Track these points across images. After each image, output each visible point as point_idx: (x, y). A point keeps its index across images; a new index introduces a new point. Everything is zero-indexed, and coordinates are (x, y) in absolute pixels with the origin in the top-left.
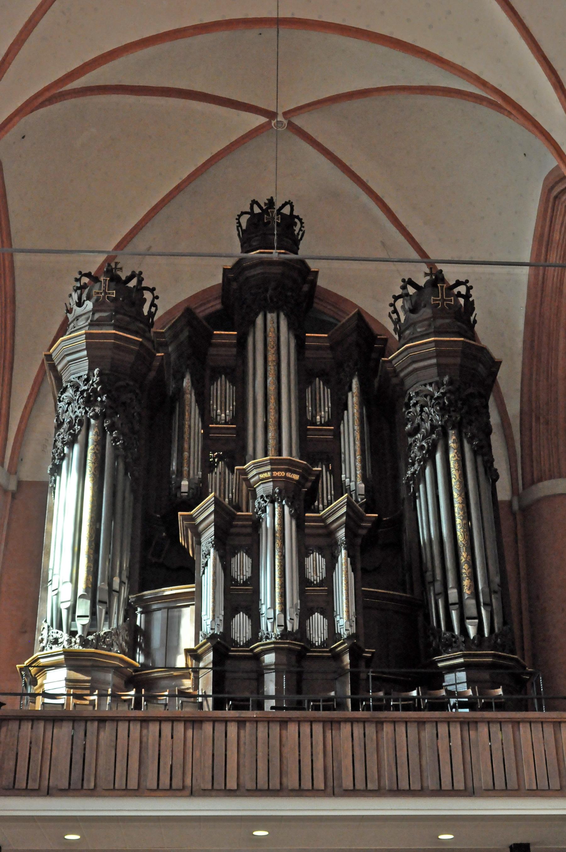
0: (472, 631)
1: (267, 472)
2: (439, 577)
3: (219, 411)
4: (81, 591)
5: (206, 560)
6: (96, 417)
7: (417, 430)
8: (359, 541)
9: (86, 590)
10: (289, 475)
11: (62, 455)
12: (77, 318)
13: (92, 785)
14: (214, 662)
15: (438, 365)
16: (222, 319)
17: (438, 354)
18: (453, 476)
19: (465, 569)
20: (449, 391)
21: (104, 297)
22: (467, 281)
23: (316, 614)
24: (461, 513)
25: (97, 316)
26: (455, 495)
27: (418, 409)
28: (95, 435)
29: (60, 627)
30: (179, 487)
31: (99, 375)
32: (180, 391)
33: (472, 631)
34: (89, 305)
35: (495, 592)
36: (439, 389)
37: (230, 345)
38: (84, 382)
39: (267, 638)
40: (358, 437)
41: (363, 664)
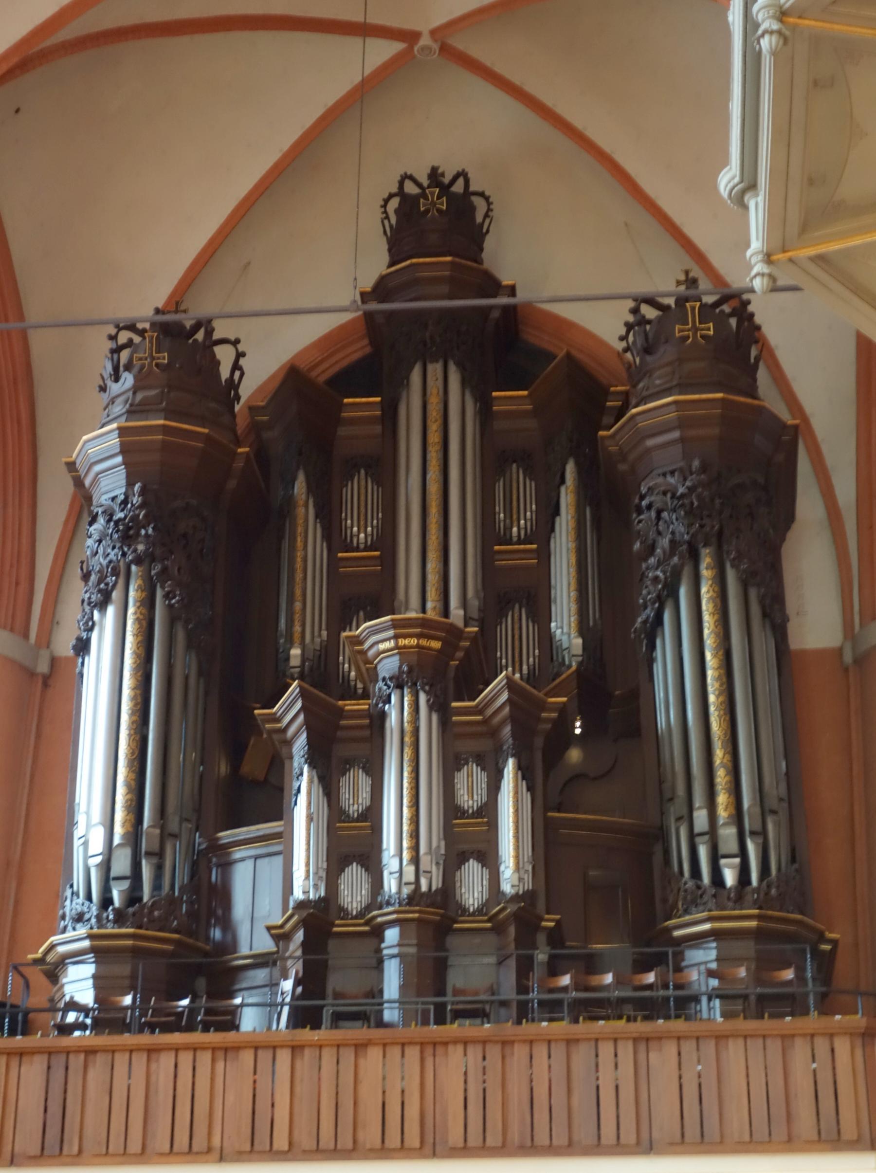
0: (730, 877)
1: (388, 639)
2: (681, 790)
3: (355, 529)
4: (117, 840)
6: (138, 561)
7: (651, 549)
8: (539, 742)
9: (125, 836)
10: (424, 642)
11: (90, 623)
13: (75, 1149)
14: (304, 944)
15: (682, 440)
16: (351, 380)
17: (682, 424)
19: (721, 776)
21: (150, 364)
23: (471, 861)
24: (717, 685)
25: (139, 396)
26: (708, 656)
27: (653, 514)
28: (137, 591)
29: (89, 898)
30: (288, 659)
31: (142, 492)
33: (730, 877)
34: (128, 379)
35: (774, 812)
36: (685, 479)
38: (120, 505)
39: (388, 903)
40: (573, 560)
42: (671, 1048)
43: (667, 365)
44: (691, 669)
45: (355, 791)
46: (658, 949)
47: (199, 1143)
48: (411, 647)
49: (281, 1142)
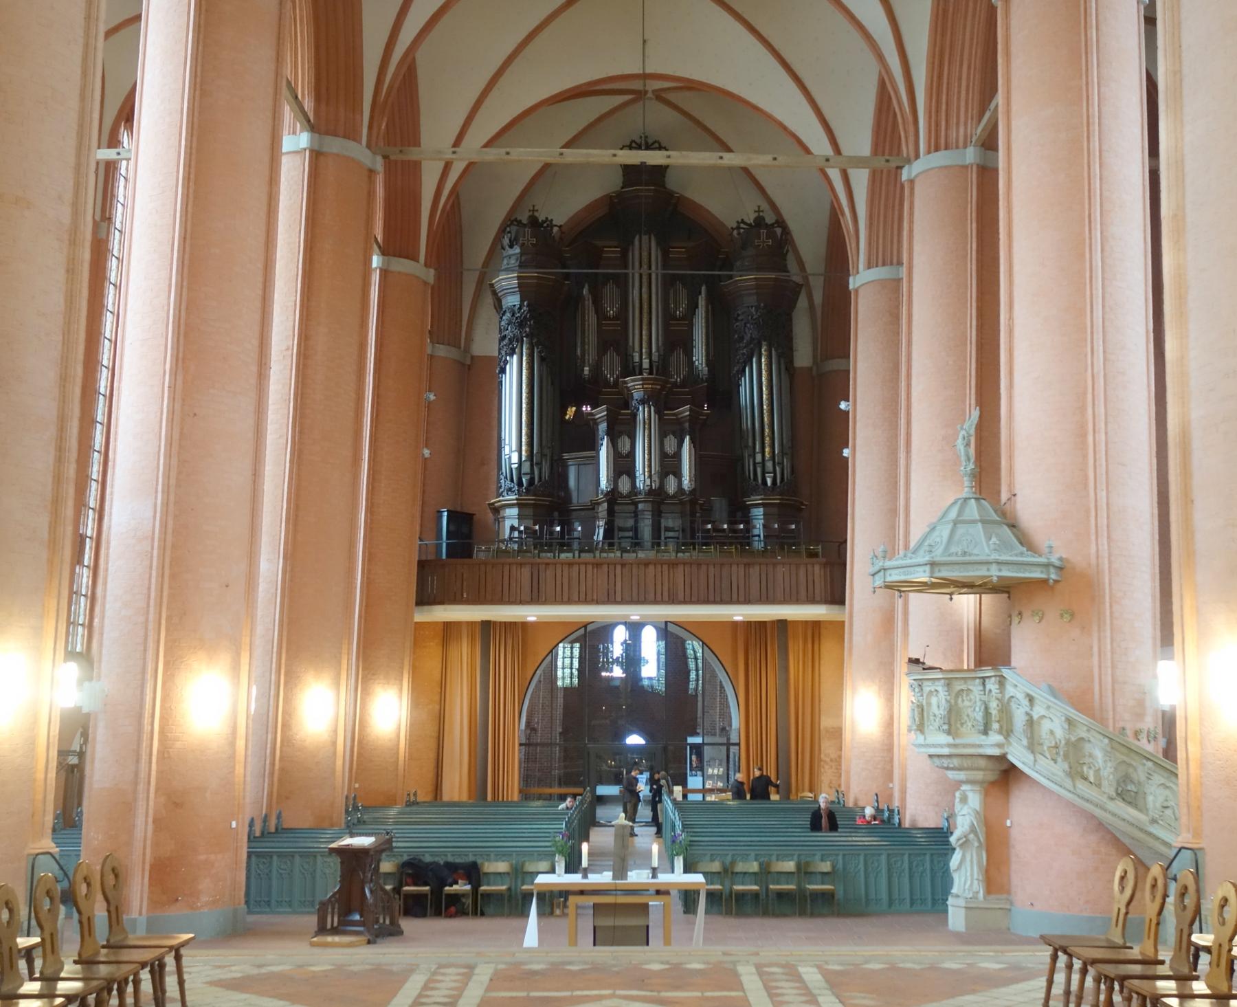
0: (769, 481)
2: (750, 444)
7: (741, 339)
12: (510, 257)
29: (512, 480)
31: (528, 305)
32: (580, 297)
33: (769, 481)
34: (517, 250)
41: (698, 507)
42: (757, 568)
44: (755, 387)
45: (624, 444)
46: (740, 512)
47: (589, 597)
49: (619, 599)
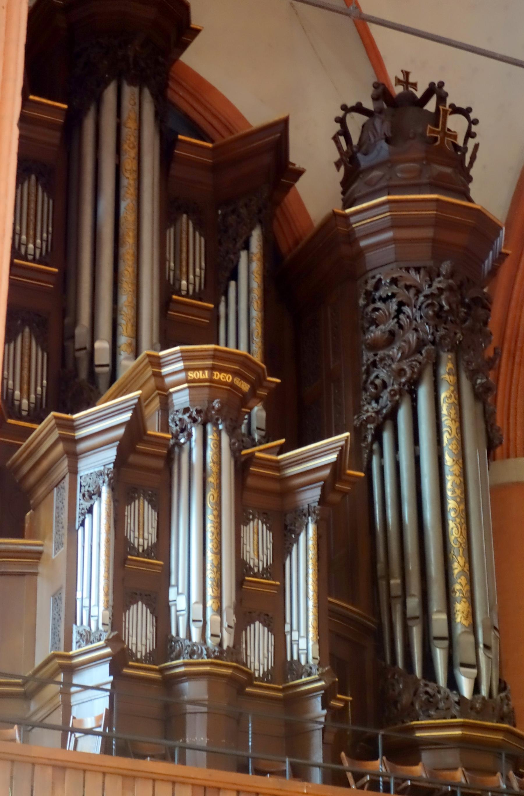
1: (203, 369)
3: (24, 237)
5: (92, 502)
10: (238, 382)
18: (445, 429)
19: (459, 586)
20: (450, 288)
22: (469, 110)
27: (394, 307)
36: (432, 280)
37: (50, 125)
43: (414, 161)
48: (226, 384)
